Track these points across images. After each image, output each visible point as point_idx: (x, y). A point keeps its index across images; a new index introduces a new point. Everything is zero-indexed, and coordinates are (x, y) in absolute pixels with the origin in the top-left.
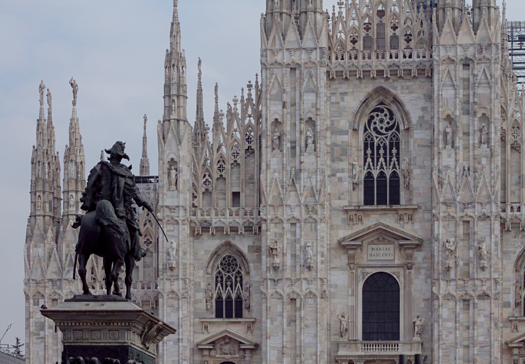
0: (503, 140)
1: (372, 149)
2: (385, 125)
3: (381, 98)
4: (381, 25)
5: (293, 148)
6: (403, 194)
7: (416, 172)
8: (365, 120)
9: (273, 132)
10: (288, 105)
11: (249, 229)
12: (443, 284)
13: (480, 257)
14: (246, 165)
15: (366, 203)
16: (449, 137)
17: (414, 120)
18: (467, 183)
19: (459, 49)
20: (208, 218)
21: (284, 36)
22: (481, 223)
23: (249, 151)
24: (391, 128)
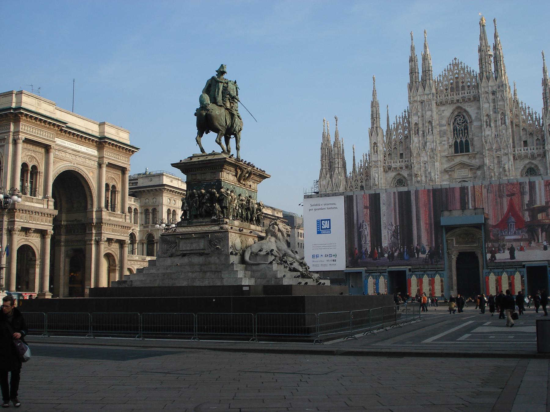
0: (512, 122)
1: (457, 131)
2: (461, 121)
3: (459, 111)
4: (457, 83)
5: (423, 133)
6: (471, 148)
7: (475, 138)
11: (407, 167)
13: (505, 171)
15: (455, 153)
16: (488, 123)
17: (473, 118)
18: (497, 141)
19: (490, 88)
20: (390, 164)
21: (417, 90)
22: (505, 157)
24: (464, 122)
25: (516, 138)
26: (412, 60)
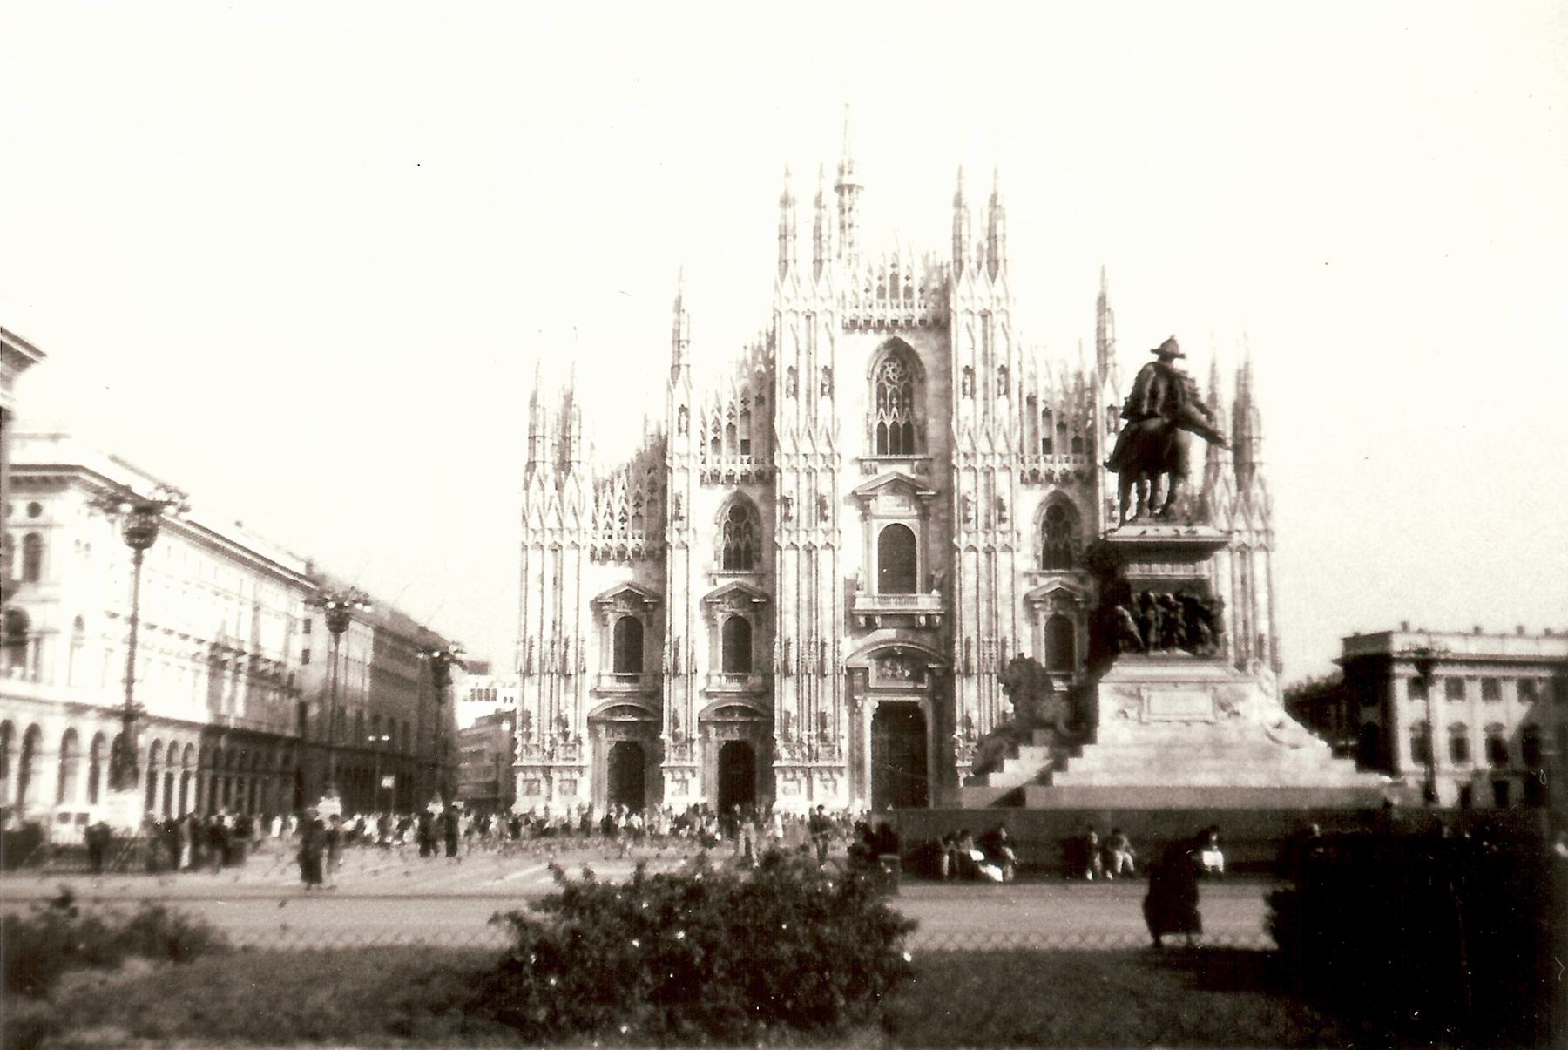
7: (931, 421)
8: (877, 370)
16: (968, 388)
23: (760, 400)
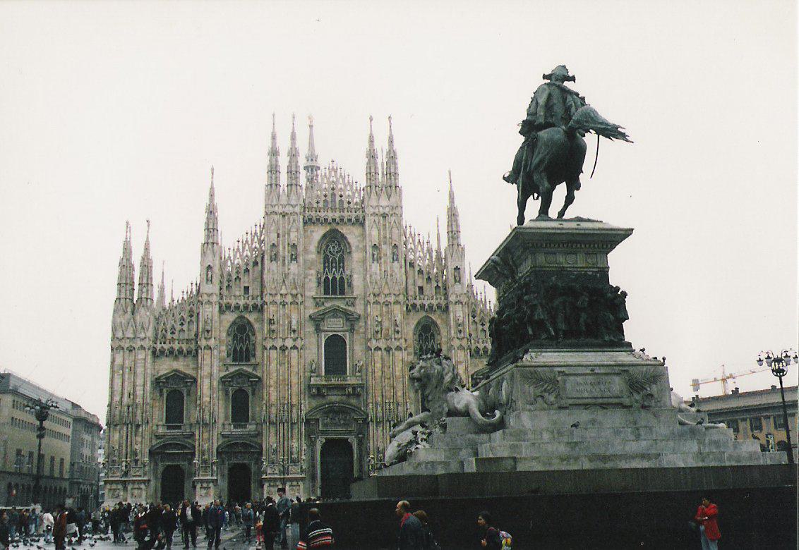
4: (334, 195)
7: (355, 276)
9: (272, 251)
10: (281, 236)
12: (374, 341)
14: (253, 271)
23: (256, 263)
25: (410, 281)
26: (274, 153)
